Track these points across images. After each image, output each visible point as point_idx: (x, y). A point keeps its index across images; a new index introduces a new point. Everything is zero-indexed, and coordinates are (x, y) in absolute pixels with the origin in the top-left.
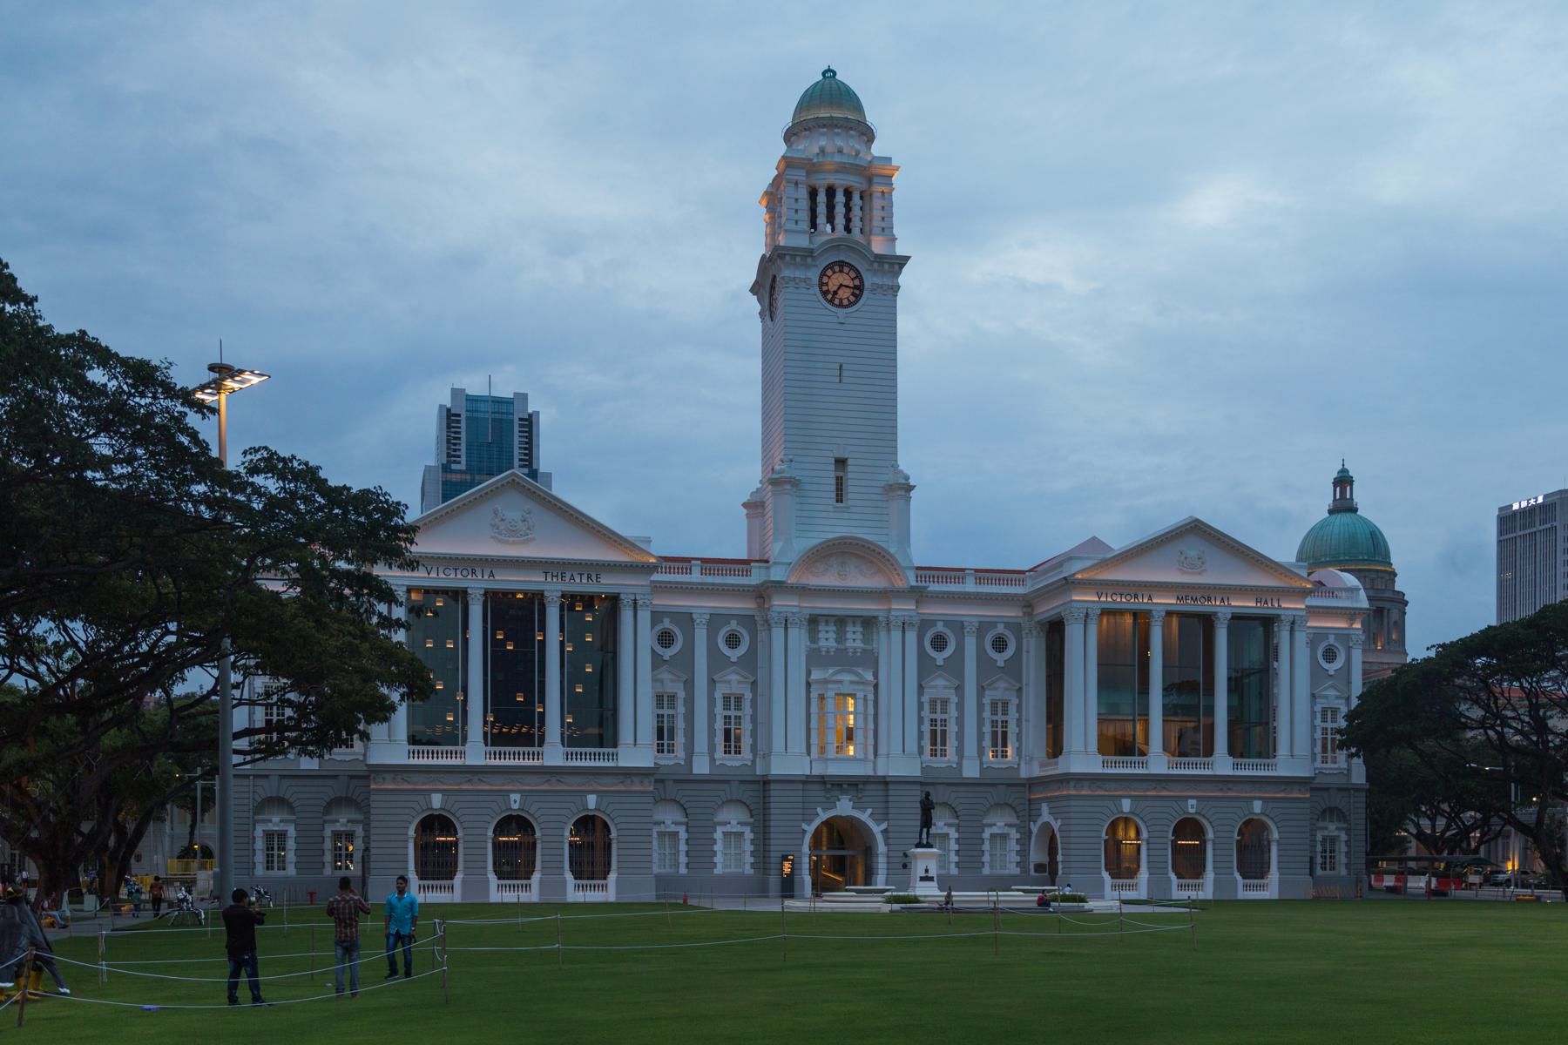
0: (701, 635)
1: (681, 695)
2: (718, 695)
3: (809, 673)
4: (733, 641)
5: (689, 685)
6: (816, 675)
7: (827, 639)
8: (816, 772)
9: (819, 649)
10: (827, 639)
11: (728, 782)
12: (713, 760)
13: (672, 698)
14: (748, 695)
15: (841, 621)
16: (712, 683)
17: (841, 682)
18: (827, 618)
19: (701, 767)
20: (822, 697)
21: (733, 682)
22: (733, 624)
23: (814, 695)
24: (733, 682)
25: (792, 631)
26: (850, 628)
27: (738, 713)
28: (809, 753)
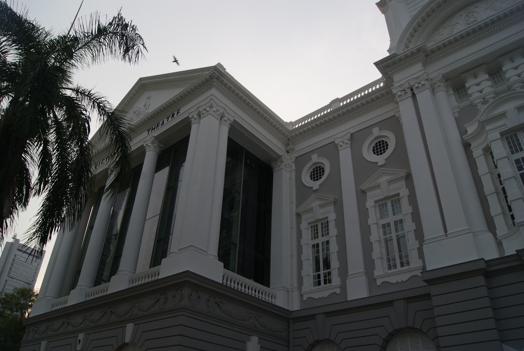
0: (345, 156)
1: (332, 217)
2: (370, 203)
3: (463, 132)
4: (380, 147)
5: (338, 204)
6: (471, 129)
7: (480, 87)
8: (510, 250)
9: (473, 107)
10: (480, 87)
11: (390, 303)
12: (371, 280)
13: (326, 225)
14: (404, 192)
15: (493, 67)
16: (362, 194)
17: (503, 115)
18: (472, 69)
19: (358, 291)
20: (488, 151)
21: (385, 185)
22: (376, 132)
23: (477, 153)
24: (385, 185)
25: (424, 97)
26: (507, 67)
27: (398, 217)
28: (491, 227)
